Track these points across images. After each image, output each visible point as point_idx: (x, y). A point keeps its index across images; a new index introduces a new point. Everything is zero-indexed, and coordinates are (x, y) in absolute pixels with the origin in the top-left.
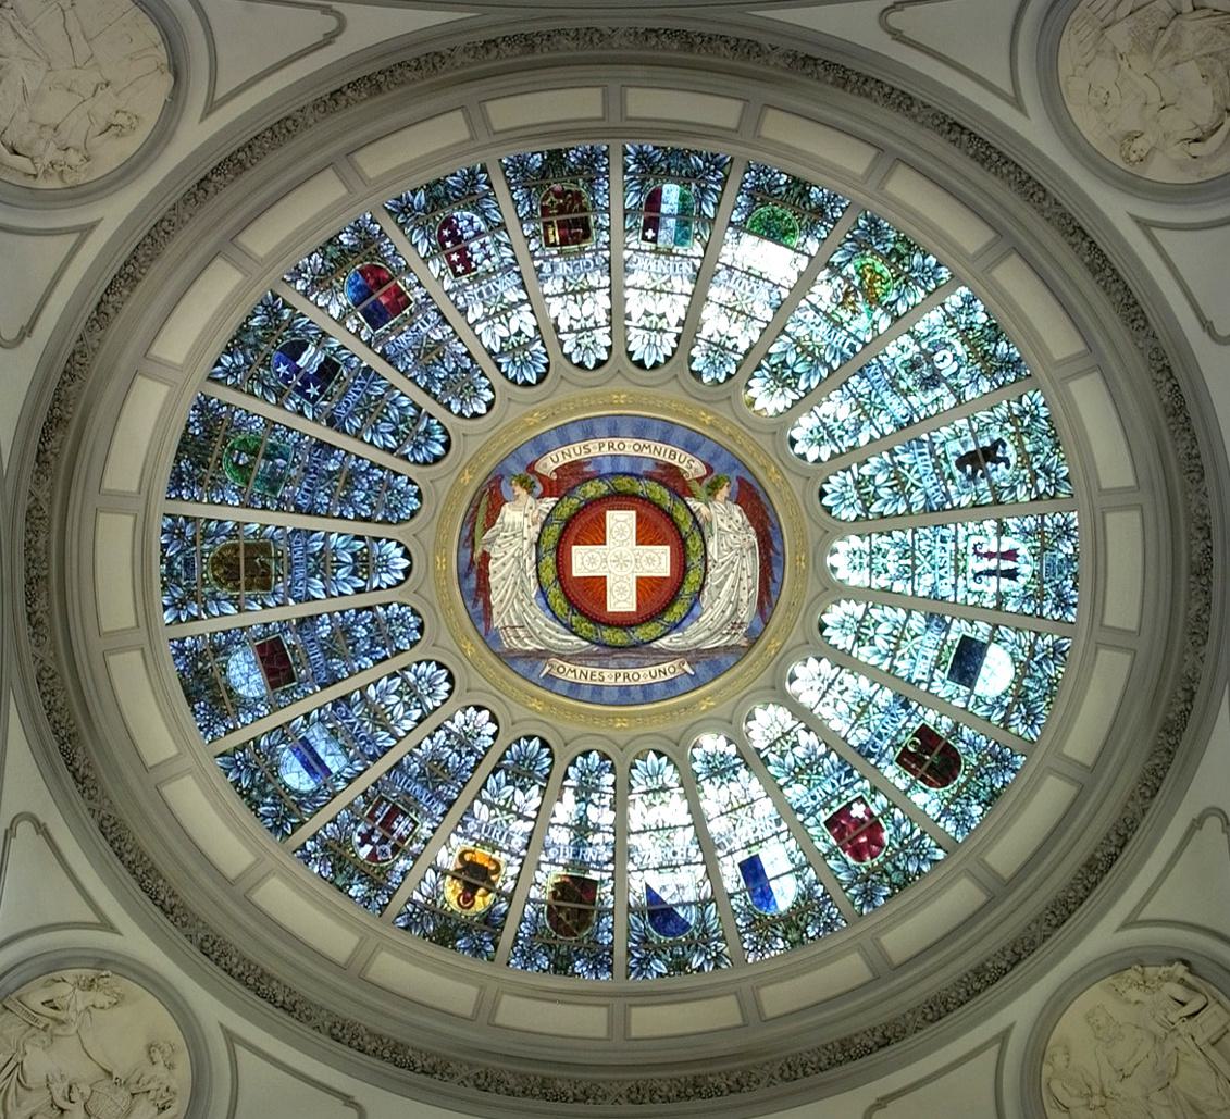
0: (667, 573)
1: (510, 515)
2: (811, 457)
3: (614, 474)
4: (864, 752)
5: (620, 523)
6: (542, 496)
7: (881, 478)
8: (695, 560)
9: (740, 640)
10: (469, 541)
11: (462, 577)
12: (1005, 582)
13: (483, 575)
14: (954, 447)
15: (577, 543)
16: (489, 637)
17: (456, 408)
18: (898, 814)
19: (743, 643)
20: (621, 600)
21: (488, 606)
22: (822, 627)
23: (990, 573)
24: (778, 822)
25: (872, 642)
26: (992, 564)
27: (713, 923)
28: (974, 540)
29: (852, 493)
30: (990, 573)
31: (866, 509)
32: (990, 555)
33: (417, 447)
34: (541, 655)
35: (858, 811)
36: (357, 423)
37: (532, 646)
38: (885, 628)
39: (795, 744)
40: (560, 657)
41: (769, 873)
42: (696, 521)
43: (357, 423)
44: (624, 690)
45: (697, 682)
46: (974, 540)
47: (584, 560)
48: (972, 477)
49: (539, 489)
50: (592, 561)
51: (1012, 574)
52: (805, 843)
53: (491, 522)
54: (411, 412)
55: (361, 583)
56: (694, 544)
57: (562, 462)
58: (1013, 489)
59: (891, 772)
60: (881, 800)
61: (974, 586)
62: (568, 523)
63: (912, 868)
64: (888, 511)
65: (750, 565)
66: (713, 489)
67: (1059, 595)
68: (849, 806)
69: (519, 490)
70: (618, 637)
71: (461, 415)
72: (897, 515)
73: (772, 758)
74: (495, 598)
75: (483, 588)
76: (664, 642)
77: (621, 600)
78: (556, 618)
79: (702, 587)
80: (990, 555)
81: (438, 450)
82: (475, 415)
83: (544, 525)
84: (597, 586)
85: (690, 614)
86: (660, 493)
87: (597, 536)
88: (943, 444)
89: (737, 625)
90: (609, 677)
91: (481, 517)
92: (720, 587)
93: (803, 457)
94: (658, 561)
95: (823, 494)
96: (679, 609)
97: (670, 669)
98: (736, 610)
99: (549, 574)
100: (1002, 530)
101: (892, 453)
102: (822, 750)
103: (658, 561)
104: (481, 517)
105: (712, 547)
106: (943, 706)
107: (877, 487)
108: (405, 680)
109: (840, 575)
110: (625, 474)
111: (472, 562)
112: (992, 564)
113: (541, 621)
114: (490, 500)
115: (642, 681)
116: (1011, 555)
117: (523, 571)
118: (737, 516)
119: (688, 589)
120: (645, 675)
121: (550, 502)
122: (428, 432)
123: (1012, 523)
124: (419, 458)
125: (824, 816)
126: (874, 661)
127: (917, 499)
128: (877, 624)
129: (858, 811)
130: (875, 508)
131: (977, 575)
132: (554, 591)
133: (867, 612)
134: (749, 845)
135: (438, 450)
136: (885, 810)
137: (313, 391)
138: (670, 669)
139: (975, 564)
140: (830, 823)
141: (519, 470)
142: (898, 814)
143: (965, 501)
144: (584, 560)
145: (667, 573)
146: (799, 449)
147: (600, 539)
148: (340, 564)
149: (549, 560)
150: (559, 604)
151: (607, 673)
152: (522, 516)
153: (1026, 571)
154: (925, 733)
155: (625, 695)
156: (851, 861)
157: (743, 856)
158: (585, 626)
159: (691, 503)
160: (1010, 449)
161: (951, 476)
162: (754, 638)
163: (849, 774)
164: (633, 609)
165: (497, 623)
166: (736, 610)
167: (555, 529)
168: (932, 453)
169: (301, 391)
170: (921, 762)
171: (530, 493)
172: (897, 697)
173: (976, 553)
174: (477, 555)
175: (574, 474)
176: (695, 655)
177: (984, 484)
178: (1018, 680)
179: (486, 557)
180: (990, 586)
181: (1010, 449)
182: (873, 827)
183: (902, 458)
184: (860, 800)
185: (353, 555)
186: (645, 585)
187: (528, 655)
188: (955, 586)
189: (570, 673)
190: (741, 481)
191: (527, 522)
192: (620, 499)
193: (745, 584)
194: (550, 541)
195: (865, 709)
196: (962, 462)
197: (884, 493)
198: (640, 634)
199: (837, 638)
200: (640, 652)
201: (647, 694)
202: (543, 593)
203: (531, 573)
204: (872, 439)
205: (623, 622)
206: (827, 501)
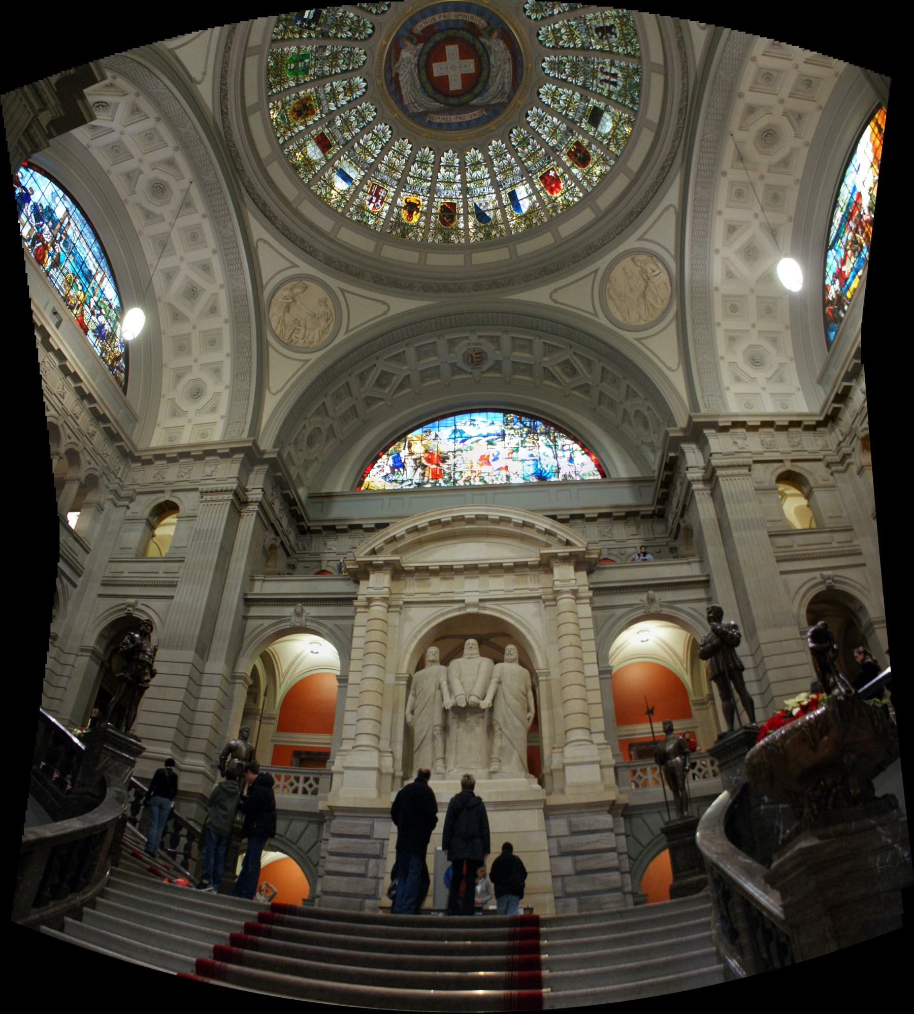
0: (473, 71)
1: (405, 54)
2: (533, 17)
3: (447, 29)
4: (554, 149)
5: (452, 50)
6: (416, 44)
7: (563, 31)
8: (484, 66)
9: (505, 100)
10: (389, 69)
11: (388, 85)
12: (612, 86)
13: (397, 82)
14: (594, 22)
15: (435, 61)
16: (404, 109)
17: (374, 11)
18: (567, 176)
19: (507, 101)
20: (455, 85)
21: (401, 97)
22: (539, 94)
23: (606, 81)
24: (522, 177)
25: (559, 103)
26: (608, 77)
27: (499, 217)
28: (601, 66)
29: (551, 36)
30: (606, 81)
31: (557, 43)
32: (607, 73)
33: (361, 33)
34: (426, 113)
35: (552, 173)
36: (334, 31)
37: (421, 110)
38: (563, 97)
39: (529, 144)
40: (433, 113)
41: (519, 197)
42: (484, 48)
43: (334, 31)
44: (460, 124)
45: (489, 119)
46: (601, 66)
47: (438, 69)
48: (601, 38)
49: (415, 40)
50: (442, 69)
51: (615, 84)
52: (532, 185)
53: (397, 59)
54: (356, 18)
55: (349, 98)
56: (484, 59)
57: (424, 26)
58: (618, 48)
59: (564, 158)
60: (561, 170)
61: (600, 85)
62: (429, 55)
63: (571, 199)
64: (566, 45)
65: (508, 67)
66: (490, 35)
67: (632, 98)
68: (548, 172)
69: (408, 43)
70: (455, 101)
71: (377, 13)
72: (569, 47)
73: (519, 149)
74: (404, 92)
75: (398, 89)
76: (474, 102)
77: (455, 85)
78: (430, 96)
79: (488, 77)
80: (607, 73)
81: (370, 31)
82: (383, 12)
83: (420, 56)
84: (444, 80)
85: (485, 88)
86: (468, 36)
87: (442, 57)
88: (590, 20)
89: (504, 94)
90: (453, 119)
91: (393, 59)
92: (497, 75)
93: (529, 17)
94: (469, 66)
95: (538, 35)
96: (479, 87)
97: (476, 114)
98: (503, 87)
99: (424, 78)
100: (612, 64)
101: (568, 21)
102: (538, 147)
103: (469, 66)
104: (393, 59)
105: (492, 59)
106: (585, 133)
107: (562, 35)
108: (373, 133)
109: (547, 71)
110: (452, 29)
111: (392, 79)
112: (608, 77)
113: (424, 99)
114: (396, 48)
115: (467, 119)
116: (615, 76)
117: (413, 77)
118: (502, 45)
119: (483, 79)
120: (467, 117)
121: (421, 46)
122: (364, 24)
123: (617, 62)
124: (362, 37)
125: (539, 174)
126: (559, 110)
127: (578, 42)
128: (561, 95)
129: (552, 173)
130: (561, 43)
131: (602, 81)
132: (428, 86)
133: (557, 89)
134: (511, 186)
135: (370, 31)
136: (562, 175)
137: (313, 26)
138: (476, 114)
139: (601, 76)
140: (542, 178)
141: (406, 34)
142: (567, 176)
143: (598, 47)
144: (438, 69)
145: (473, 71)
146: (527, 13)
147: (444, 59)
148: (339, 93)
149: (423, 72)
150: (430, 90)
151: (452, 117)
152: (408, 54)
153: (620, 84)
154: (578, 144)
155: (460, 126)
156: (549, 194)
157: (509, 190)
158: (442, 98)
159: (482, 40)
160: (617, 30)
161: (593, 35)
162: (510, 98)
163: (549, 158)
164: (460, 88)
165: (406, 103)
166: (503, 87)
167: (424, 57)
168: (585, 23)
169: (309, 28)
170: (576, 156)
171: (412, 43)
172: (568, 127)
173: (601, 71)
174: (394, 74)
175: (430, 31)
176: (487, 106)
177: (606, 42)
178: (614, 129)
179: (397, 75)
180: (607, 87)
181: (617, 30)
182: (556, 180)
183: (573, 23)
184: (553, 169)
185: (344, 88)
186: (465, 77)
187: (420, 114)
188: (592, 84)
189: (438, 119)
190: (503, 29)
191: (412, 56)
192: (451, 40)
193: (506, 75)
194: (422, 63)
195: (555, 131)
196: (598, 30)
197: (565, 37)
198: (464, 99)
199: (544, 99)
200: (465, 107)
201: (469, 125)
202: (423, 86)
203: (417, 78)
204: (559, 12)
205: (456, 94)
206: (540, 38)
